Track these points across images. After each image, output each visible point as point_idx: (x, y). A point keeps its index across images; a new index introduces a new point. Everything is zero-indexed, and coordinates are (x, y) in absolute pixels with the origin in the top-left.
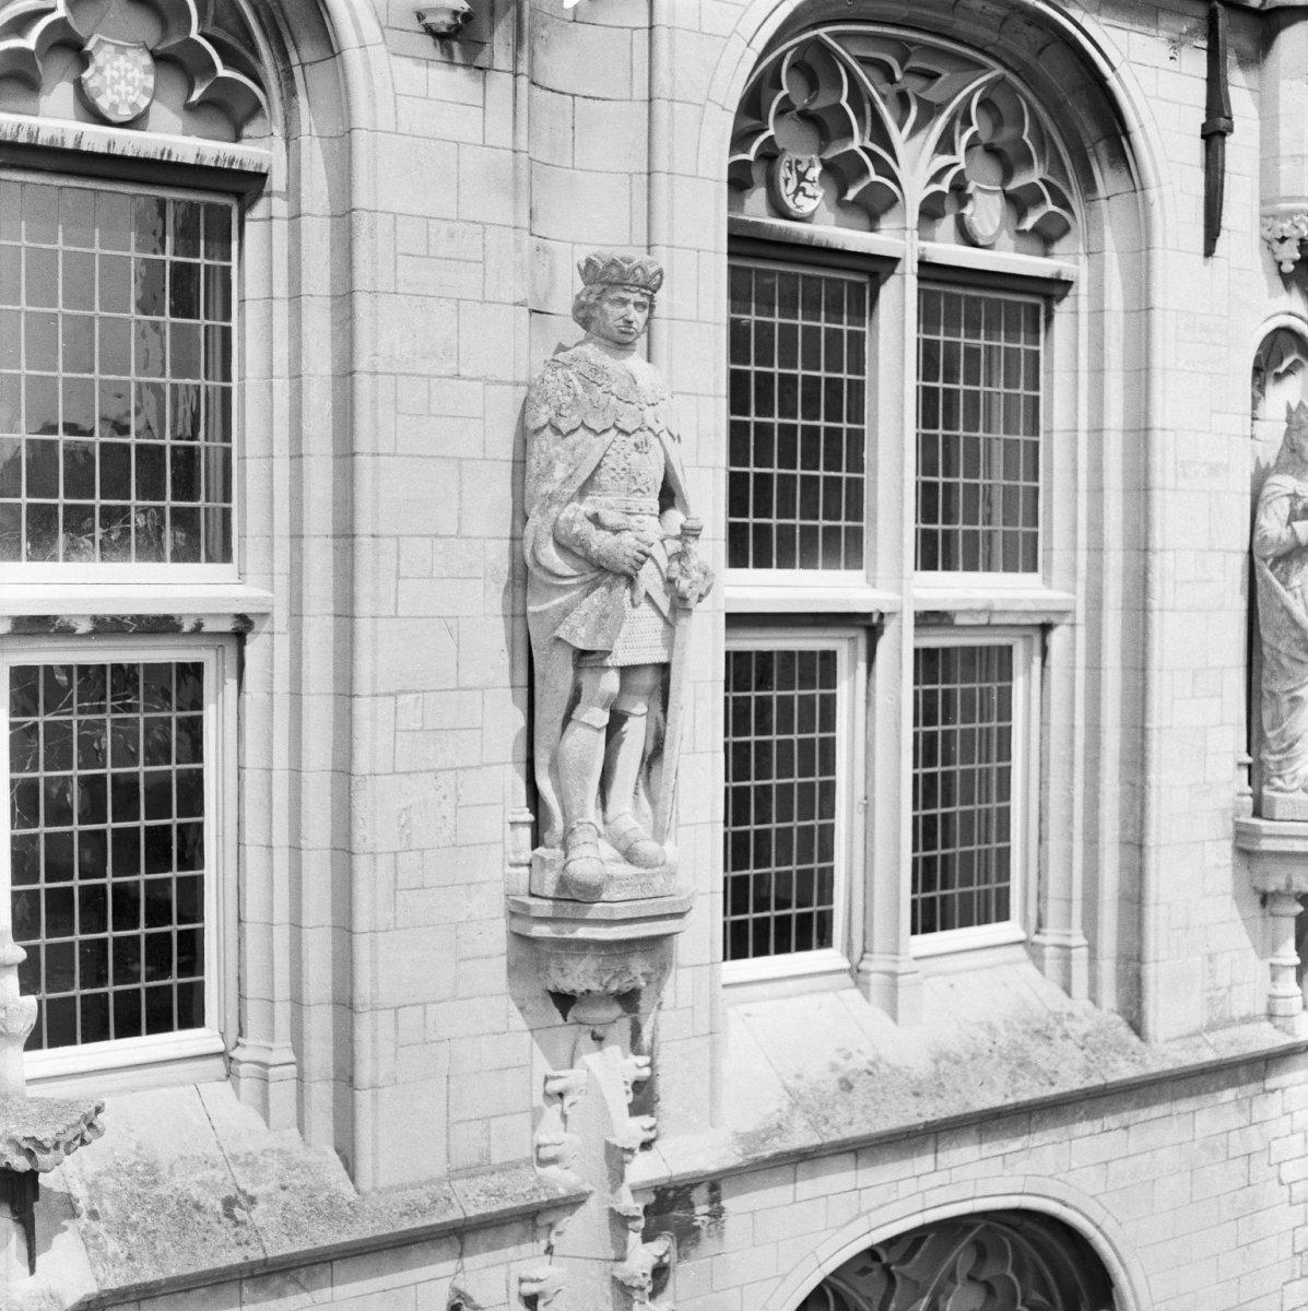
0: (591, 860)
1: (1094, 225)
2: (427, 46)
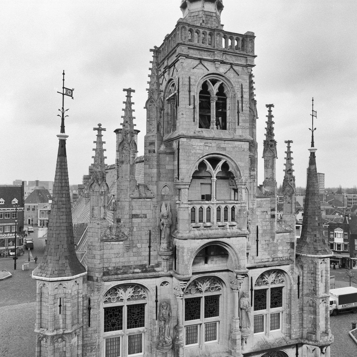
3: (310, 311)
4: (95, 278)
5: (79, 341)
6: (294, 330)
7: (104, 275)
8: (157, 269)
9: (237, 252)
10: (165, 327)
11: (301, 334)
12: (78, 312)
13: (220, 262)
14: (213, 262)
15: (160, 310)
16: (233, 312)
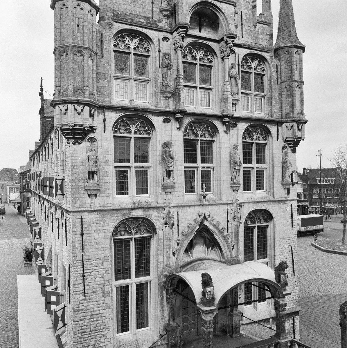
0: (235, 181)
1: (269, 139)
2: (224, 133)
3: (288, 95)
4: (106, 17)
5: (94, 66)
6: (275, 111)
7: (114, 16)
8: (159, 24)
9: (227, 17)
10: (167, 73)
11: (281, 115)
12: (93, 40)
13: (212, 33)
14: (206, 32)
15: (162, 60)
16: (224, 78)
